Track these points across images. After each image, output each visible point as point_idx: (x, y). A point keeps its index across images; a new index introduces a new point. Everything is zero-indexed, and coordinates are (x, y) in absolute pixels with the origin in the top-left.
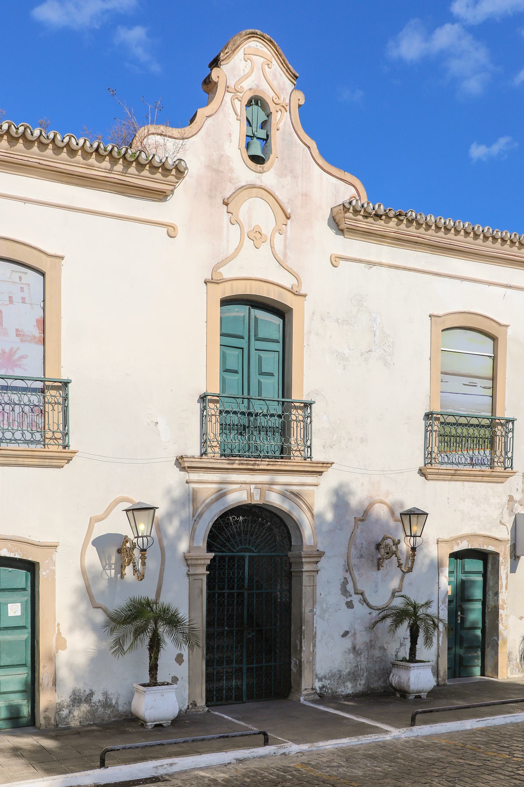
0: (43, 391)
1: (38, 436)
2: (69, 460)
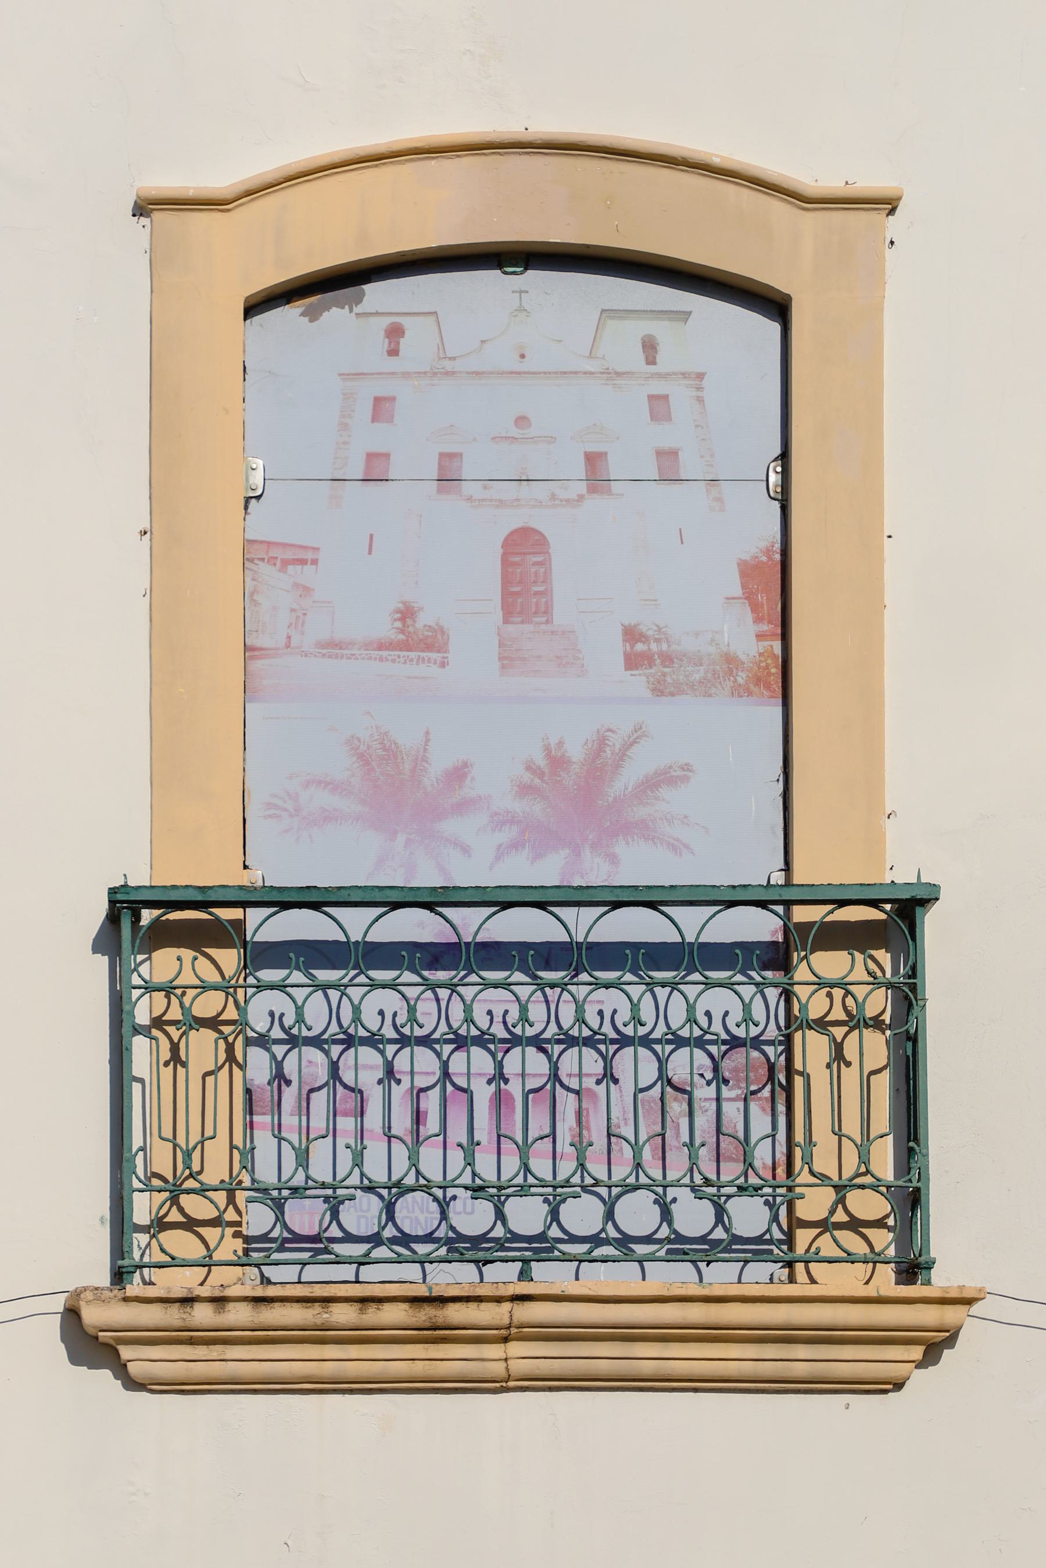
0: (777, 957)
1: (749, 1217)
2: (935, 1347)
